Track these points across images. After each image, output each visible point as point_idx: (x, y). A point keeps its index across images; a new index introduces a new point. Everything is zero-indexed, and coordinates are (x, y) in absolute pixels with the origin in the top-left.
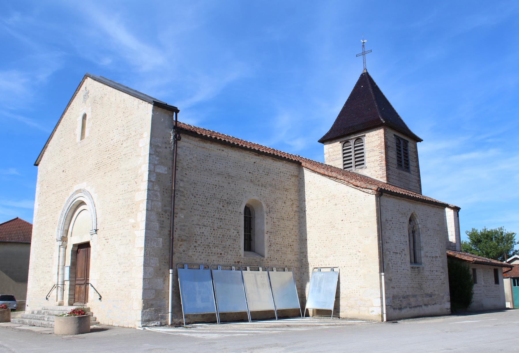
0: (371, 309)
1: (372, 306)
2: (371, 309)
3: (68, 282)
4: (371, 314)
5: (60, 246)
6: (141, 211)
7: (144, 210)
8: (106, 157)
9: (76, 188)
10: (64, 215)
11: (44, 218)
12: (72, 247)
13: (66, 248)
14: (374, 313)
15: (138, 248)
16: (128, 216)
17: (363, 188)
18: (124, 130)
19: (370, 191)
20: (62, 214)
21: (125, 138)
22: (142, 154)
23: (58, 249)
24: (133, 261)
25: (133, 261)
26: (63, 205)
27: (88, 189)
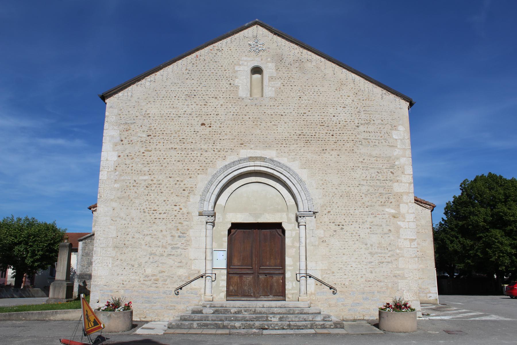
0: (429, 295)
1: (430, 292)
2: (429, 295)
3: (225, 272)
4: (430, 299)
5: (207, 223)
6: (407, 203)
7: (410, 202)
8: (324, 132)
9: (244, 153)
10: (215, 184)
11: (146, 177)
12: (230, 226)
13: (214, 226)
14: (431, 298)
15: (405, 239)
16: (382, 205)
17: (422, 203)
18: (359, 112)
19: (428, 206)
20: (211, 183)
21: (363, 122)
22: (399, 146)
23: (204, 226)
24: (398, 251)
25: (398, 251)
26: (211, 171)
27: (284, 161)
